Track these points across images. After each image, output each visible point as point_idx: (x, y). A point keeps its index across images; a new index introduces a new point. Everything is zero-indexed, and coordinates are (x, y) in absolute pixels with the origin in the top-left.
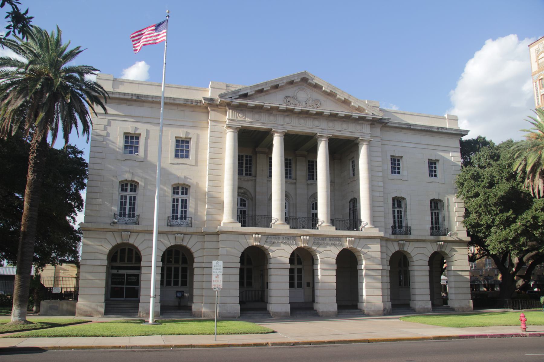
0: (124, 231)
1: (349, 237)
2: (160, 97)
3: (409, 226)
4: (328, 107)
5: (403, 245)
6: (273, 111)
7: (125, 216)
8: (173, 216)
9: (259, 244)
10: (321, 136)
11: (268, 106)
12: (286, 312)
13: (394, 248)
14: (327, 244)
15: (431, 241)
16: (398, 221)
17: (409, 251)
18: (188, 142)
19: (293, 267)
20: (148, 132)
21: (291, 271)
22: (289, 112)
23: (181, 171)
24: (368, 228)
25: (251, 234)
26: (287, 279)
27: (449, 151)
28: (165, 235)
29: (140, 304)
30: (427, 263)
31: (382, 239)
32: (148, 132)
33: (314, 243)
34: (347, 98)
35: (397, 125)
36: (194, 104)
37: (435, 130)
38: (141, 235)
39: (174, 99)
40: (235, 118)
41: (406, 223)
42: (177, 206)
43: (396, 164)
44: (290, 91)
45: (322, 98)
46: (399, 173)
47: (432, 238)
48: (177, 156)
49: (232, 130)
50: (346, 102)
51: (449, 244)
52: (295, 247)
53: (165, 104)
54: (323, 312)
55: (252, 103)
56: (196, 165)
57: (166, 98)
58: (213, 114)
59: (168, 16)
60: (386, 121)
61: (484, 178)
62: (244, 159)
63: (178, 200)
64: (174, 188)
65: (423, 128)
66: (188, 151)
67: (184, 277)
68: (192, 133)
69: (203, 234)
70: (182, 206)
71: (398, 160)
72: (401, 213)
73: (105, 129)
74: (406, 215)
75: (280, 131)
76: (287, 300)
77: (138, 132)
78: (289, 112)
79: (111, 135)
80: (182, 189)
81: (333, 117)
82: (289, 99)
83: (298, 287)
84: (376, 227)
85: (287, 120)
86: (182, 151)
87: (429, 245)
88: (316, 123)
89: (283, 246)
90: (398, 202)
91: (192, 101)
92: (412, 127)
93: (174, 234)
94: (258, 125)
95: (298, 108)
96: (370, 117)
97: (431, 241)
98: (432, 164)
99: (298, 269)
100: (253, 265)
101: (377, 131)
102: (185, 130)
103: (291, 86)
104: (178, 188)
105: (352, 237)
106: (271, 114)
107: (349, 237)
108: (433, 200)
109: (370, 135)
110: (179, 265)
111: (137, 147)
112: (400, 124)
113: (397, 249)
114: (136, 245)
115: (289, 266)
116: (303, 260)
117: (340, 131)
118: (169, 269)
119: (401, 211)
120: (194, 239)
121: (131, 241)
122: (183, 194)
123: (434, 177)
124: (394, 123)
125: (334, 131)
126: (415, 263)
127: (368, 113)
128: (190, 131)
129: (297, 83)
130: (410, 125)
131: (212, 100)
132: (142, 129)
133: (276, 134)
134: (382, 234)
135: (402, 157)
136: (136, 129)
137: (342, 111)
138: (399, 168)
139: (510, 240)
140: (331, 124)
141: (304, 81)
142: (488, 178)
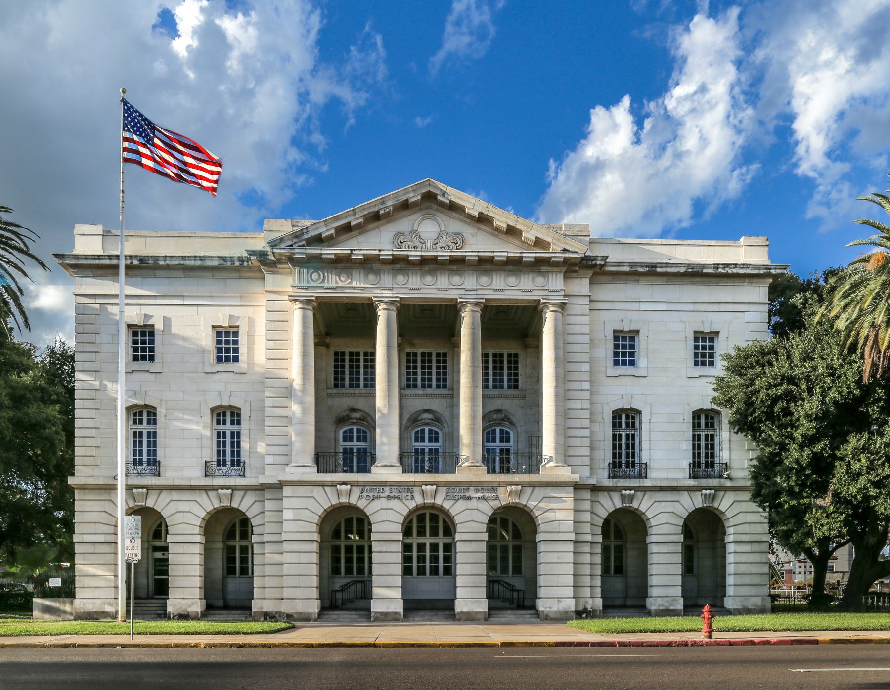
9: (517, 501)
13: (609, 504)
15: (689, 489)
17: (643, 508)
28: (203, 493)
38: (164, 494)
41: (641, 457)
43: (625, 347)
46: (632, 363)
47: (692, 483)
52: (412, 505)
63: (224, 433)
74: (641, 442)
83: (431, 574)
86: (228, 350)
90: (626, 420)
97: (689, 489)
99: (431, 544)
113: (619, 505)
120: (165, 497)
122: (232, 423)
126: (653, 531)
135: (638, 332)
138: (632, 355)
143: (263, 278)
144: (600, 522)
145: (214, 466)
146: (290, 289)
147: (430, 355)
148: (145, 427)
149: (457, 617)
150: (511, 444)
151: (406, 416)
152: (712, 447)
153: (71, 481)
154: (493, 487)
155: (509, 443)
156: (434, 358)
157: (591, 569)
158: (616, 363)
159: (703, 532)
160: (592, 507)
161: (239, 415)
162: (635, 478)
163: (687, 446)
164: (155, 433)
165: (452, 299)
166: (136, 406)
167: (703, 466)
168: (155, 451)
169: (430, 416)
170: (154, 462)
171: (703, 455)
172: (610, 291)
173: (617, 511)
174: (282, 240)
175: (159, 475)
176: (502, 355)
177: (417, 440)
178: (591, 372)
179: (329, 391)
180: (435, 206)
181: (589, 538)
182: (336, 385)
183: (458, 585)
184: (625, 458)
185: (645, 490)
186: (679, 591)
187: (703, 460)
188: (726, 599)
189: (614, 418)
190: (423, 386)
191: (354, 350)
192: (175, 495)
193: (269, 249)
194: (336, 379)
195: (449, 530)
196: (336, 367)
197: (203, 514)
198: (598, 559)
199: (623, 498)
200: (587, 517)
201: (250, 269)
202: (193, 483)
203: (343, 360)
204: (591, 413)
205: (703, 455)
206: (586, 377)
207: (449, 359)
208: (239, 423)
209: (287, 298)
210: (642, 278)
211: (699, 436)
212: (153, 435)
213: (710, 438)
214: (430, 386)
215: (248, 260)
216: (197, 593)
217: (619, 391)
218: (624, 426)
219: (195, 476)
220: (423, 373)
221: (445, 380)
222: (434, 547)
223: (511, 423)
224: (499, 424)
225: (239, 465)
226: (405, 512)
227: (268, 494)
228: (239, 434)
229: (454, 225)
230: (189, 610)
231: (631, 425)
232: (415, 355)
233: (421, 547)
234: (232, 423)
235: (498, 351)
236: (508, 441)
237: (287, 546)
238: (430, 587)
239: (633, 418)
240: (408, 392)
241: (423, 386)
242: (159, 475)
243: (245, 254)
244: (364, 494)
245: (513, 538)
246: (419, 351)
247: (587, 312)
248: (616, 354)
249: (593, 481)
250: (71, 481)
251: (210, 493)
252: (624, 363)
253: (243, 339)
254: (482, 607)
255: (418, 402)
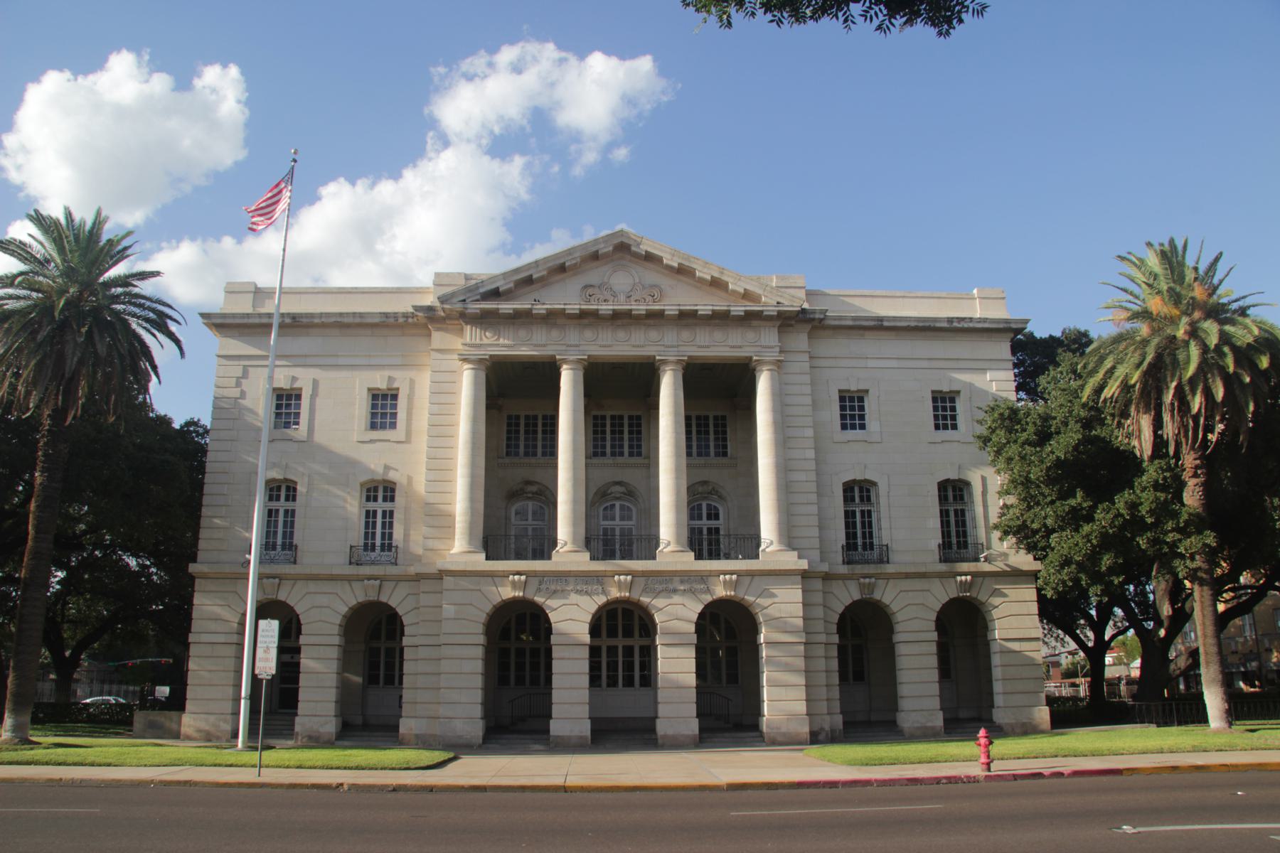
0: (369, 579)
1: (725, 573)
2: (270, 315)
3: (884, 543)
4: (677, 298)
5: (871, 588)
6: (552, 318)
7: (274, 548)
8: (366, 545)
10: (664, 362)
11: (540, 309)
12: (581, 737)
13: (847, 595)
14: (675, 591)
16: (864, 534)
17: (886, 600)
18: (395, 397)
19: (597, 642)
20: (315, 383)
21: (594, 651)
22: (587, 318)
23: (376, 457)
24: (772, 553)
25: (505, 575)
26: (585, 666)
27: (984, 370)
28: (346, 584)
29: (297, 719)
30: (932, 626)
31: (805, 575)
32: (315, 383)
33: (645, 591)
34: (716, 275)
35: (850, 323)
36: (401, 320)
37: (945, 325)
38: (300, 584)
39: (361, 315)
40: (478, 341)
41: (880, 538)
42: (374, 523)
43: (852, 409)
44: (594, 275)
45: (665, 282)
46: (863, 427)
47: (943, 567)
48: (373, 426)
49: (470, 366)
50: (717, 284)
51: (987, 580)
52: (602, 600)
53: (282, 326)
54: (665, 736)
55: (506, 307)
56: (408, 440)
57: (283, 315)
58: (439, 338)
59: (295, 161)
60: (817, 316)
61: (1027, 423)
62: (694, 423)
63: (375, 512)
64: (368, 490)
65: (913, 324)
66: (394, 415)
67: (390, 666)
68: (401, 380)
69: (419, 578)
70: (384, 524)
71: (861, 399)
72: (870, 516)
73: (238, 384)
74: (879, 520)
75: (572, 358)
76: (584, 711)
77: (297, 385)
78: (587, 318)
79: (248, 396)
80: (381, 491)
81: (687, 318)
82: (590, 291)
83: (624, 686)
84: (794, 549)
85: (588, 334)
87: (936, 585)
88: (653, 334)
89: (574, 598)
90: (859, 493)
91: (395, 315)
92: (886, 324)
93: (360, 579)
94: (525, 351)
95: (605, 308)
96: (771, 310)
98: (943, 400)
100: (517, 639)
101: (800, 340)
102: (387, 373)
103: (596, 263)
104: (376, 489)
105: (731, 573)
106: (555, 325)
107: (725, 573)
108: (947, 480)
109: (778, 349)
110: (376, 640)
111: (298, 415)
112: (855, 319)
113: (857, 596)
114: (291, 602)
115: (587, 639)
116: (623, 630)
117: (708, 347)
118: (504, 653)
119: (869, 512)
121: (282, 596)
122: (385, 499)
123: (950, 432)
124: (840, 318)
125: (695, 349)
127: (769, 303)
128: (397, 374)
129: (606, 255)
130: (881, 319)
131: (430, 309)
132: (304, 378)
133: (565, 366)
134: (804, 564)
135: (867, 391)
136: (294, 379)
137: (705, 304)
138: (862, 417)
139: (1078, 563)
140: (686, 335)
141: (622, 250)
142: (1034, 423)
143: (430, 335)
144: (836, 618)
145: (361, 552)
146: (461, 347)
147: (621, 417)
148: (282, 505)
149: (660, 741)
150: (720, 523)
151: (593, 490)
152: (964, 524)
153: (193, 568)
154: (703, 577)
155: (718, 524)
156: (626, 422)
157: (827, 677)
158: (844, 427)
159: (963, 626)
160: (824, 598)
161: (393, 490)
162: (874, 563)
163: (935, 523)
164: (293, 511)
165: (649, 357)
166: (274, 480)
167: (955, 547)
168: (292, 533)
169: (622, 489)
170: (290, 546)
171: (953, 533)
172: (832, 347)
173: (855, 603)
174: (453, 295)
175: (295, 562)
176: (707, 418)
177: (605, 518)
178: (816, 438)
179: (500, 461)
180: (629, 257)
181: (823, 638)
182: (508, 454)
183: (659, 700)
184: (860, 538)
185: (889, 577)
186: (936, 703)
187: (954, 540)
188: (994, 711)
189: (845, 491)
190: (613, 454)
191: (531, 413)
192: (312, 586)
193: (437, 304)
194: (508, 446)
195: (648, 628)
196: (509, 432)
197: (344, 610)
198: (835, 664)
199: (862, 587)
200: (819, 612)
201: (415, 325)
202: (336, 571)
203: (518, 425)
204: (818, 486)
205: (953, 533)
206: (811, 443)
207: (643, 422)
208: (392, 499)
209: (456, 357)
210: (867, 333)
211: (947, 511)
212: (290, 514)
213: (961, 514)
214: (622, 454)
215: (413, 316)
216: (330, 708)
217: (854, 458)
218: (857, 500)
219: (337, 562)
220: (613, 439)
221: (639, 446)
222: (629, 651)
223: (721, 497)
224: (705, 498)
225: (390, 550)
226: (594, 608)
227: (425, 586)
228: (392, 513)
229: (650, 276)
230: (321, 730)
231: (866, 499)
232: (604, 418)
233: (612, 650)
234: (385, 499)
235: (703, 413)
236: (717, 517)
237: (446, 651)
238: (624, 702)
239: (868, 491)
240: (595, 461)
241: (613, 454)
242: (295, 562)
243: (411, 310)
244: (543, 586)
245: (728, 637)
246: (609, 414)
247: (808, 370)
248: (843, 417)
249: (825, 568)
250: (193, 568)
251: (355, 584)
252: (853, 427)
253: (402, 403)
254: (693, 727)
255: (609, 471)
